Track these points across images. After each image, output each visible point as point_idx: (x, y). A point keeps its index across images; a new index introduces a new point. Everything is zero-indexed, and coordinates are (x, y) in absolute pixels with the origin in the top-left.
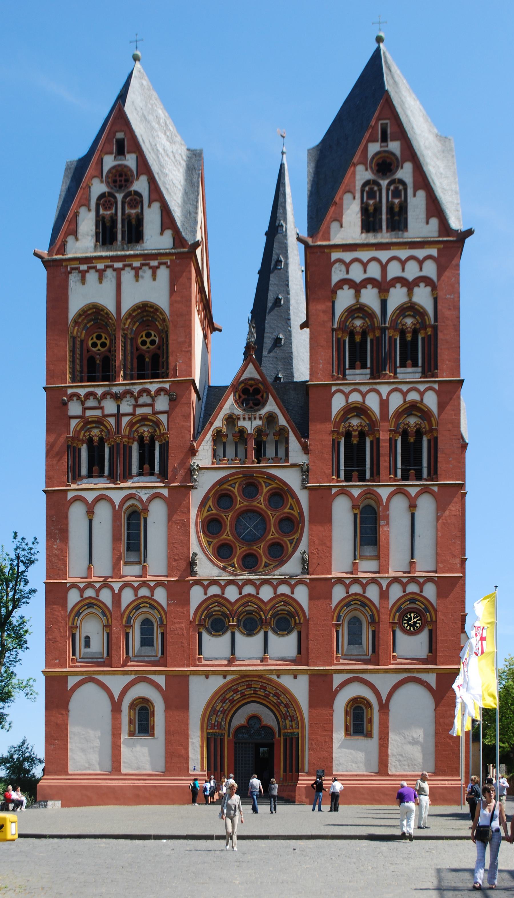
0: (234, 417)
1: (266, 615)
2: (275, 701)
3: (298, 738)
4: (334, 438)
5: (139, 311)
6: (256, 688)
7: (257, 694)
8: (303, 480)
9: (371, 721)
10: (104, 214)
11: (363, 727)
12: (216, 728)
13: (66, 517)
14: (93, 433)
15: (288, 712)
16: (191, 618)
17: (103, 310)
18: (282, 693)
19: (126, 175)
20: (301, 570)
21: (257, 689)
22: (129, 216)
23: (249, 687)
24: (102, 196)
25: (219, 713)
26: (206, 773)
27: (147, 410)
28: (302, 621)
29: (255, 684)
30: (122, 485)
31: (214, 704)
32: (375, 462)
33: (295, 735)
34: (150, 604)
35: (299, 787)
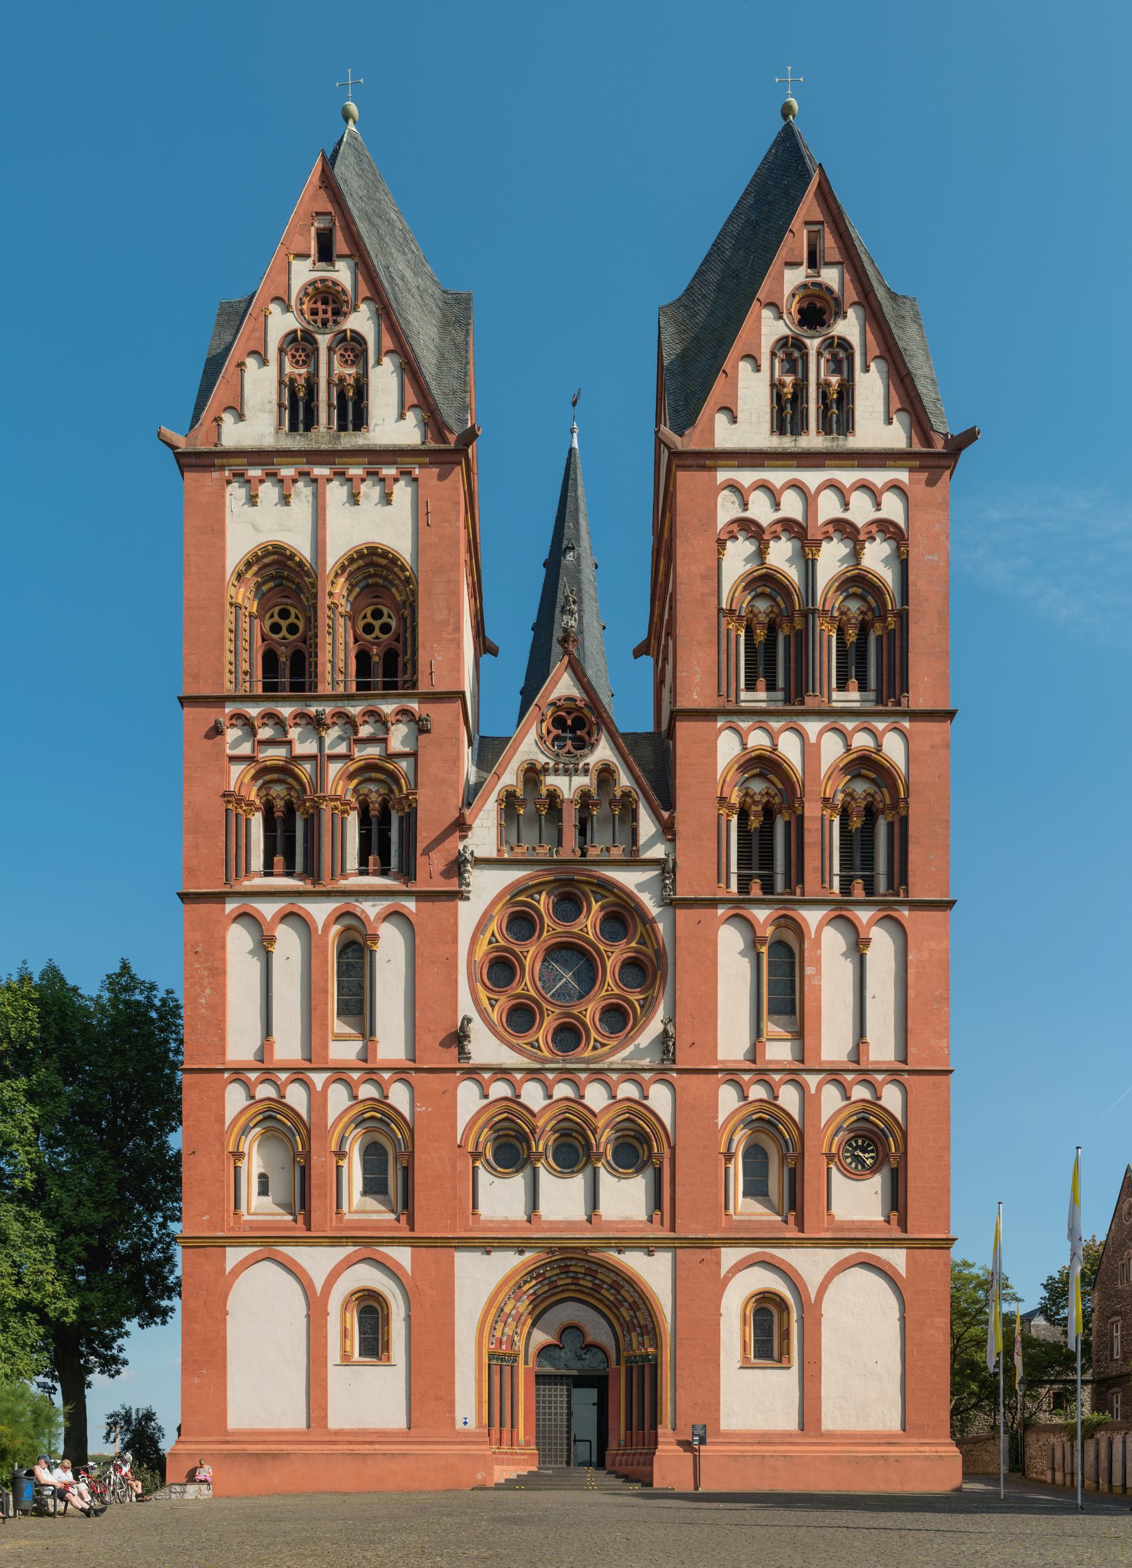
0: (539, 767)
2: (612, 1298)
4: (721, 812)
5: (361, 563)
6: (577, 1273)
8: (665, 886)
9: (786, 1335)
10: (293, 373)
11: (772, 1347)
13: (223, 947)
14: (273, 793)
15: (636, 1317)
16: (458, 1142)
17: (292, 556)
18: (628, 1282)
19: (334, 302)
20: (661, 1056)
21: (580, 1276)
22: (342, 379)
23: (565, 1270)
24: (292, 338)
27: (373, 751)
29: (576, 1265)
30: (329, 888)
32: (793, 860)
33: (650, 1360)
34: (383, 1113)
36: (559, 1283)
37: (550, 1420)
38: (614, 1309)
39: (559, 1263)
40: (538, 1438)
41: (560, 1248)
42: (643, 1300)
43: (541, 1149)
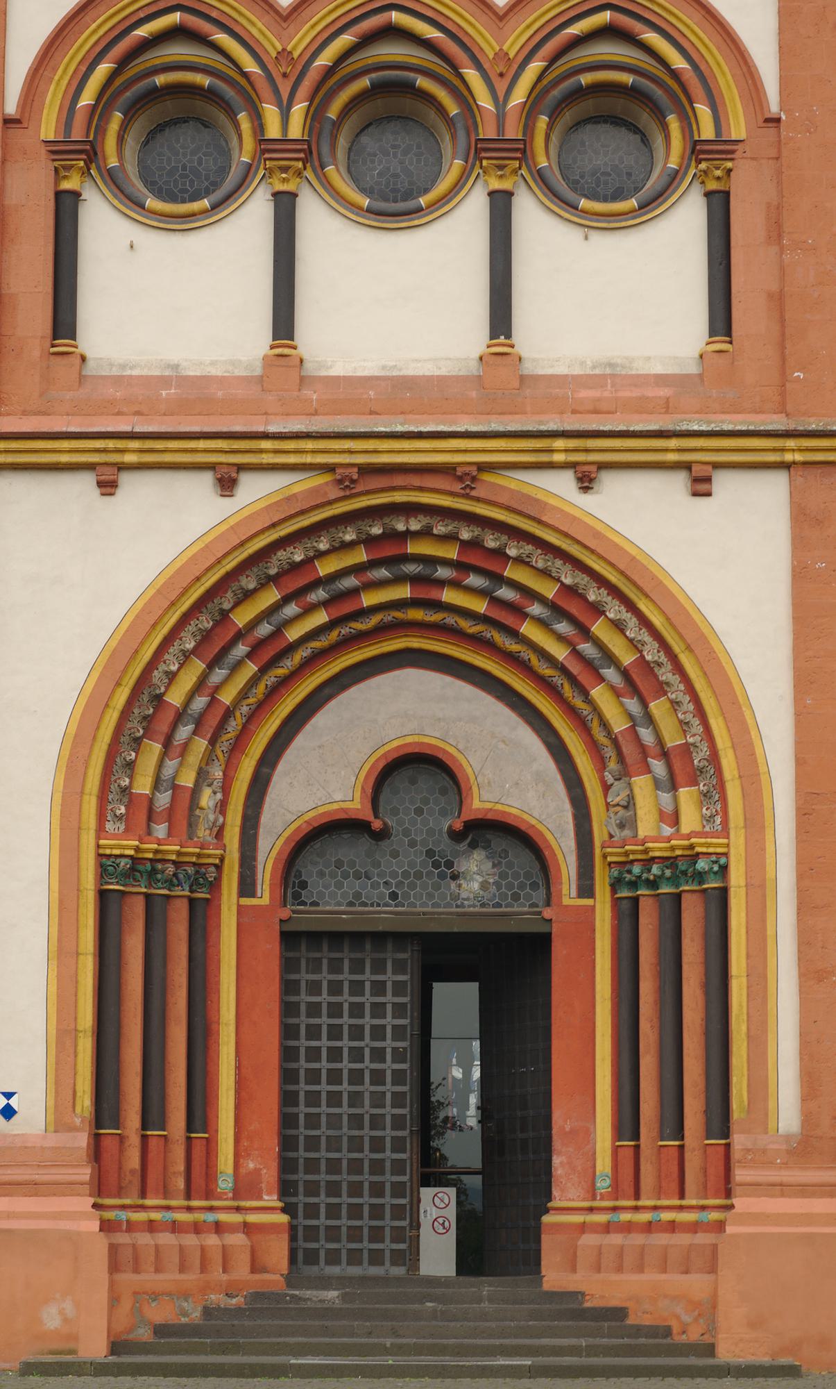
1: (501, 87)
2: (560, 653)
3: (724, 893)
7: (438, 605)
12: (160, 830)
15: (650, 720)
16: (11, 108)
18: (614, 591)
21: (443, 573)
25: (184, 732)
26: (82, 1140)
28: (738, 128)
29: (426, 533)
33: (700, 877)
35: (734, 1236)
36: (368, 600)
37: (334, 1099)
38: (568, 691)
40: (287, 1166)
41: (368, 470)
42: (673, 658)
43: (295, 131)
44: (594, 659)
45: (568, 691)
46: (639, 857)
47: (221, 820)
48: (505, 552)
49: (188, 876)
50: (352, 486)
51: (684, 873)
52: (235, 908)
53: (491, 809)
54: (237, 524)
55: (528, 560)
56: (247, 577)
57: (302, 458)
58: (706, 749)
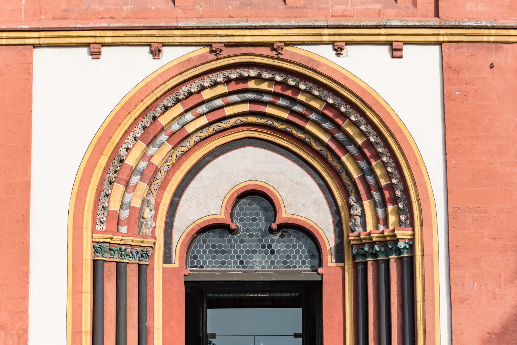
3: (412, 259)
15: (372, 172)
25: (135, 179)
31: (119, 145)
33: (399, 251)
36: (228, 111)
38: (330, 158)
39: (227, 73)
41: (228, 45)
44: (344, 141)
45: (330, 158)
46: (368, 241)
47: (154, 224)
48: (298, 87)
49: (138, 253)
50: (220, 53)
51: (391, 249)
52: (161, 269)
53: (291, 218)
54: (162, 73)
55: (310, 91)
56: (167, 100)
57: (195, 39)
58: (401, 186)
